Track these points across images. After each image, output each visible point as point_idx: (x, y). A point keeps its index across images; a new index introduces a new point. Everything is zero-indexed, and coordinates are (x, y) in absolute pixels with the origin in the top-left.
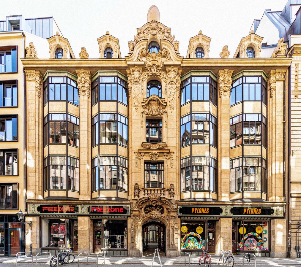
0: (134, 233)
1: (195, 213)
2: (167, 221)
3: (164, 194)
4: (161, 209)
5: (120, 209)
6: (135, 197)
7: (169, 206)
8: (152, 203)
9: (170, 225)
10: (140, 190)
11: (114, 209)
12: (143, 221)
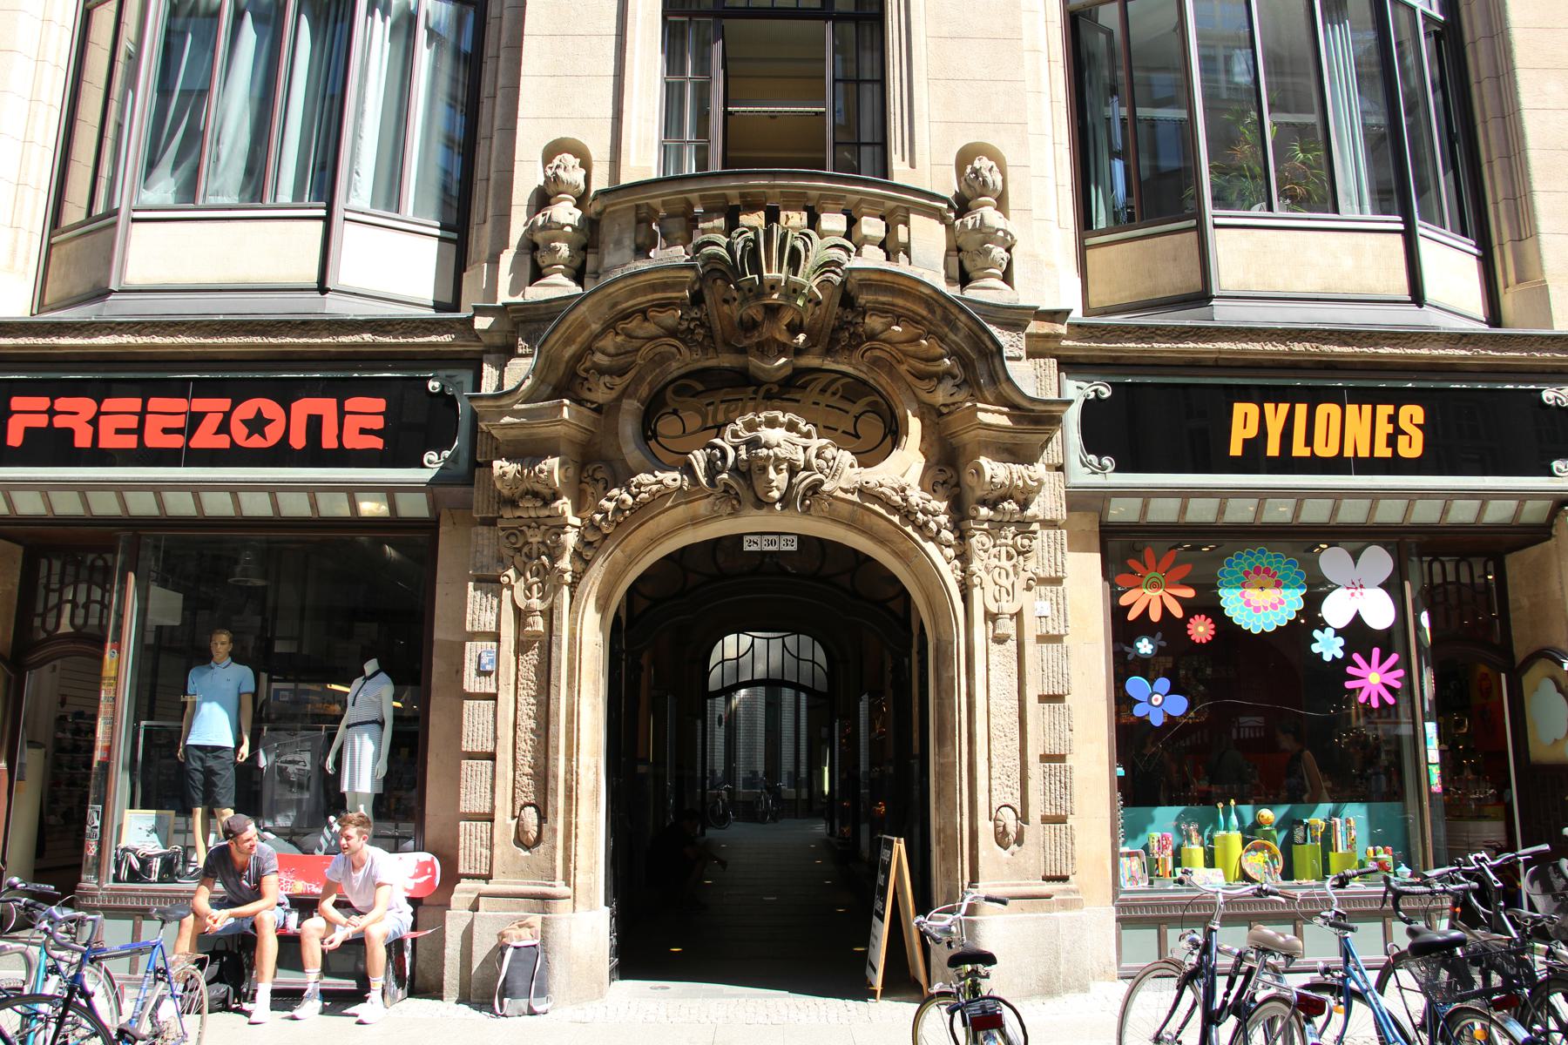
1: (1273, 449)
2: (930, 547)
3: (889, 247)
5: (342, 414)
9: (977, 592)
11: (270, 408)
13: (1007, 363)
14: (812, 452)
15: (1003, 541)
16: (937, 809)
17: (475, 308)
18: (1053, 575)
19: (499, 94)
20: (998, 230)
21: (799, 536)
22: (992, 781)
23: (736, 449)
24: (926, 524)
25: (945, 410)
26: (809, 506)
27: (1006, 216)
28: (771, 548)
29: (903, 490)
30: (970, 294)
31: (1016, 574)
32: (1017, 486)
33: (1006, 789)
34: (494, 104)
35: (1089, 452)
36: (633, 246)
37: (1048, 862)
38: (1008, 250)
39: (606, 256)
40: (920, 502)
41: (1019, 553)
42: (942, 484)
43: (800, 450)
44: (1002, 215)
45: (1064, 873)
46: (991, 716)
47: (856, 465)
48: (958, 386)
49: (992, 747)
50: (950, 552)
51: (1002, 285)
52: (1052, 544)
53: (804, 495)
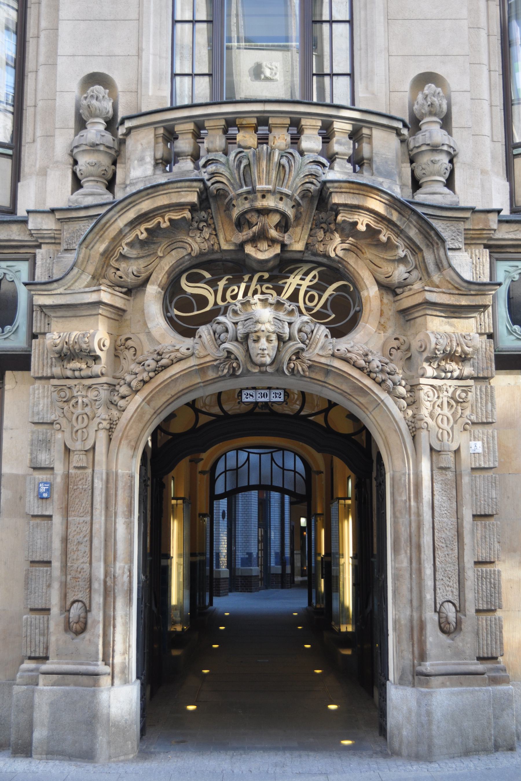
0: (57, 520)
4: (330, 290)
6: (77, 184)
7: (403, 260)
8: (247, 234)
9: (424, 434)
10: (128, 124)
12: (148, 401)
13: (450, 254)
14: (296, 326)
15: (445, 393)
16: (394, 603)
17: (28, 212)
18: (485, 421)
19: (43, 35)
20: (443, 145)
21: (285, 390)
22: (437, 583)
23: (236, 324)
24: (384, 381)
25: (399, 291)
26: (293, 369)
27: (450, 133)
28: (263, 400)
29: (367, 355)
30: (420, 197)
31: (455, 422)
32: (456, 351)
33: (447, 589)
34: (38, 42)
35: (514, 323)
36: (153, 162)
37: (481, 646)
38: (451, 161)
39: (132, 170)
40: (380, 364)
41: (457, 402)
42: (397, 350)
43: (286, 325)
44: (446, 133)
45: (495, 655)
46: (436, 531)
47: (330, 337)
48: (409, 272)
49: (437, 555)
50: (404, 403)
51: (446, 190)
52: (484, 396)
53: (290, 359)
